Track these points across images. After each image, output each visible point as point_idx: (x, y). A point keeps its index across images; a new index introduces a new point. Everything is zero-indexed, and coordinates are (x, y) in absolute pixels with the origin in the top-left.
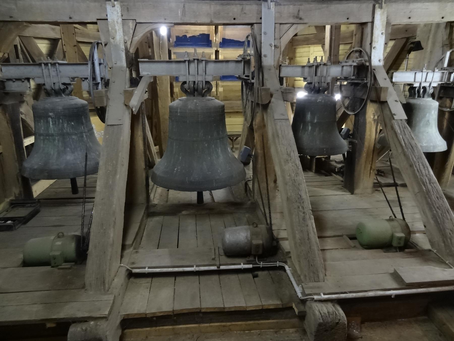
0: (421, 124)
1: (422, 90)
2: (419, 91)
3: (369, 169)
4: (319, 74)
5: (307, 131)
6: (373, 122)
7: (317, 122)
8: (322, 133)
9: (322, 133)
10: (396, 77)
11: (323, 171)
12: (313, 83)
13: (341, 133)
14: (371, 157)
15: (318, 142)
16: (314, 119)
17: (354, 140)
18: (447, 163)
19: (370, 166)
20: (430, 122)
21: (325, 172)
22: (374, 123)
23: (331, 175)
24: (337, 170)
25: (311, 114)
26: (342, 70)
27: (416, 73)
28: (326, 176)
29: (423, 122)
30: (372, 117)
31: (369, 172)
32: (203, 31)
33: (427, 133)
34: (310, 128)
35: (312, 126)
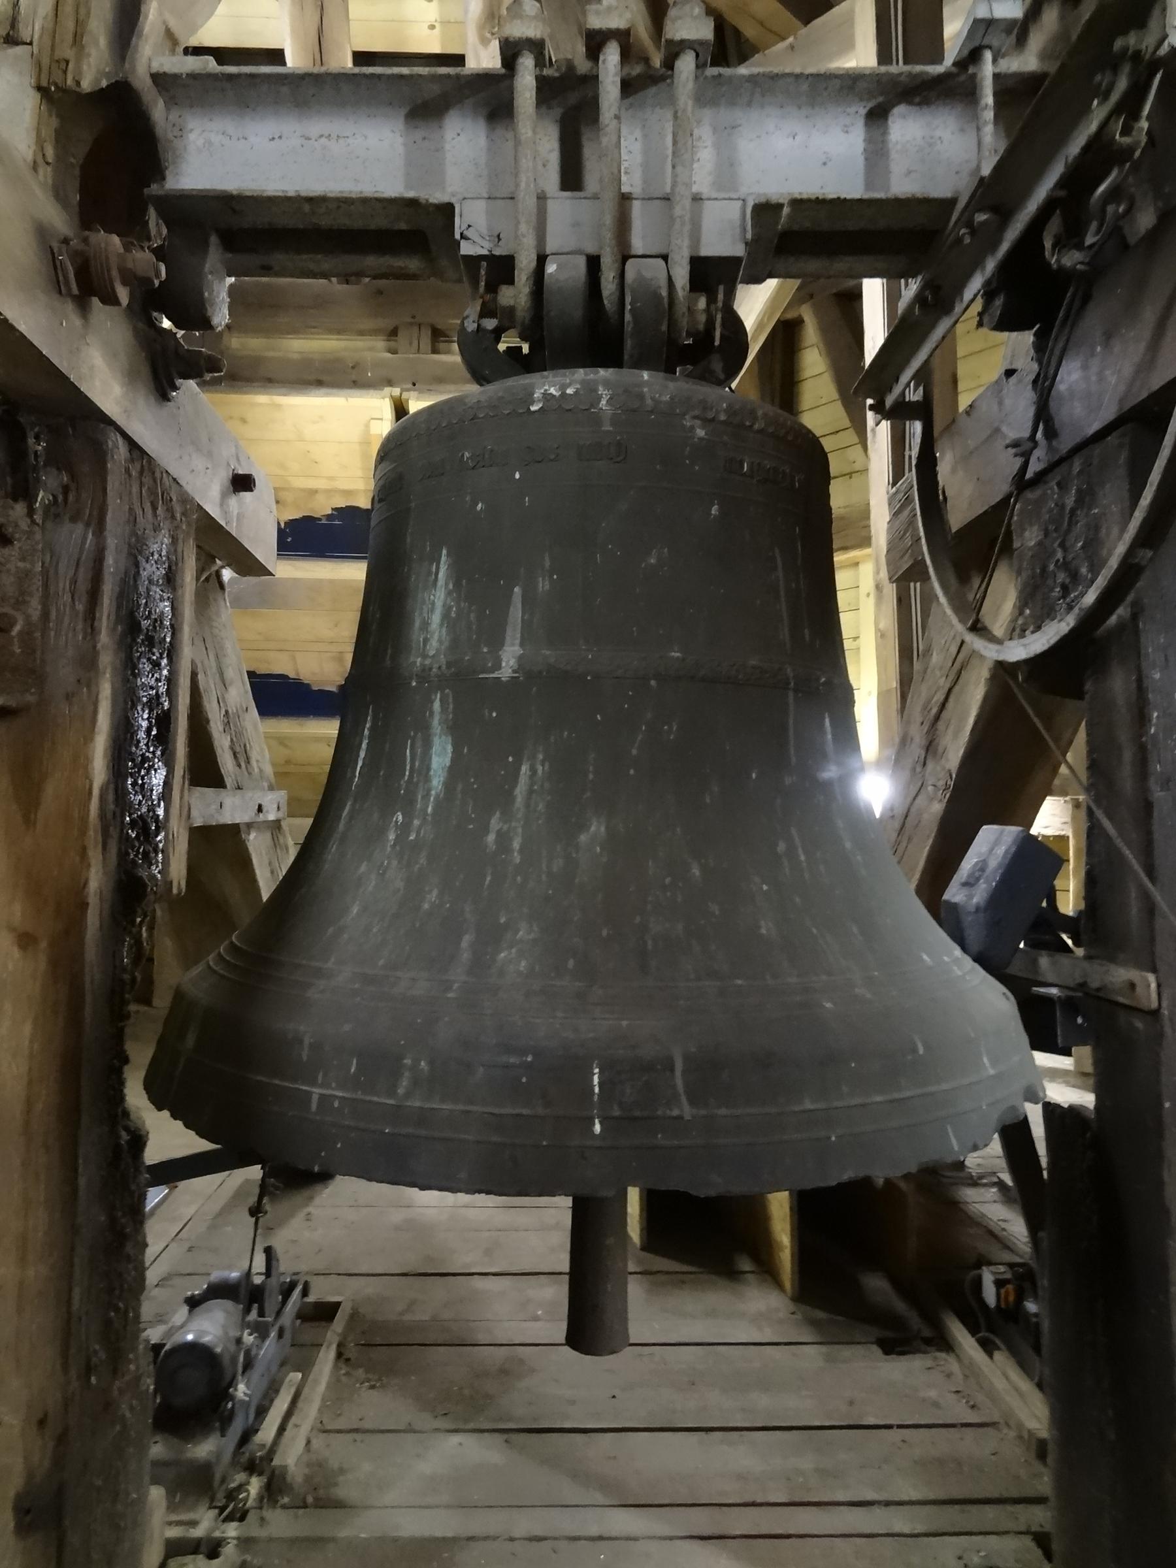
4: (593, 173)
5: (408, 805)
7: (528, 674)
8: (597, 828)
9: (597, 828)
11: (877, 1285)
12: (525, 263)
13: (954, 893)
15: (514, 960)
16: (497, 642)
17: (1121, 974)
21: (900, 1306)
23: (944, 1344)
24: (990, 1294)
25: (459, 575)
26: (876, 154)
28: (896, 1343)
32: (348, 493)
34: (441, 756)
35: (457, 730)
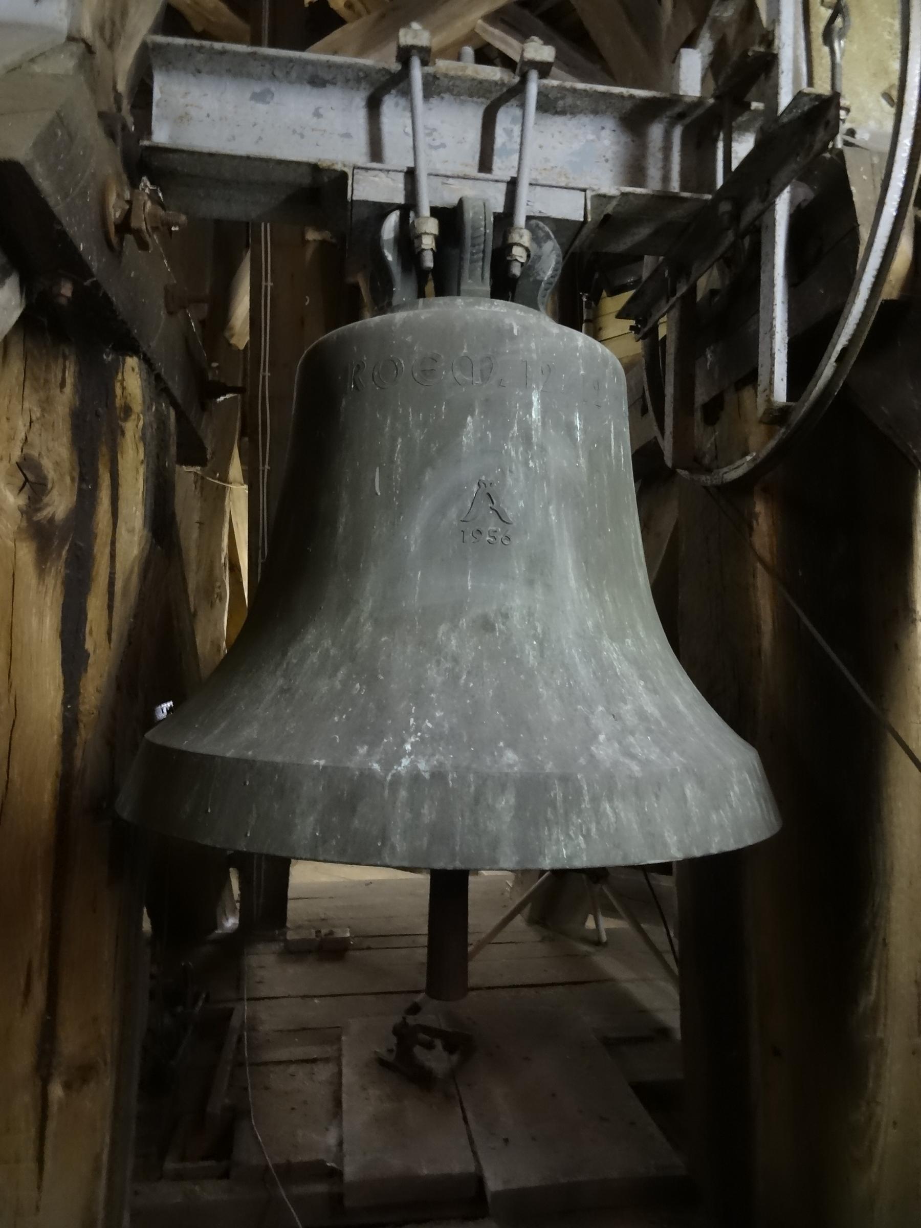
0: (414, 536)
1: (430, 227)
2: (407, 238)
3: (24, 1059)
6: (26, 554)
10: (183, 119)
14: (40, 918)
18: (867, 1001)
19: (27, 1027)
20: (515, 504)
22: (43, 556)
27: (374, 106)
29: (425, 506)
30: (13, 500)
31: (25, 1099)
33: (486, 625)
